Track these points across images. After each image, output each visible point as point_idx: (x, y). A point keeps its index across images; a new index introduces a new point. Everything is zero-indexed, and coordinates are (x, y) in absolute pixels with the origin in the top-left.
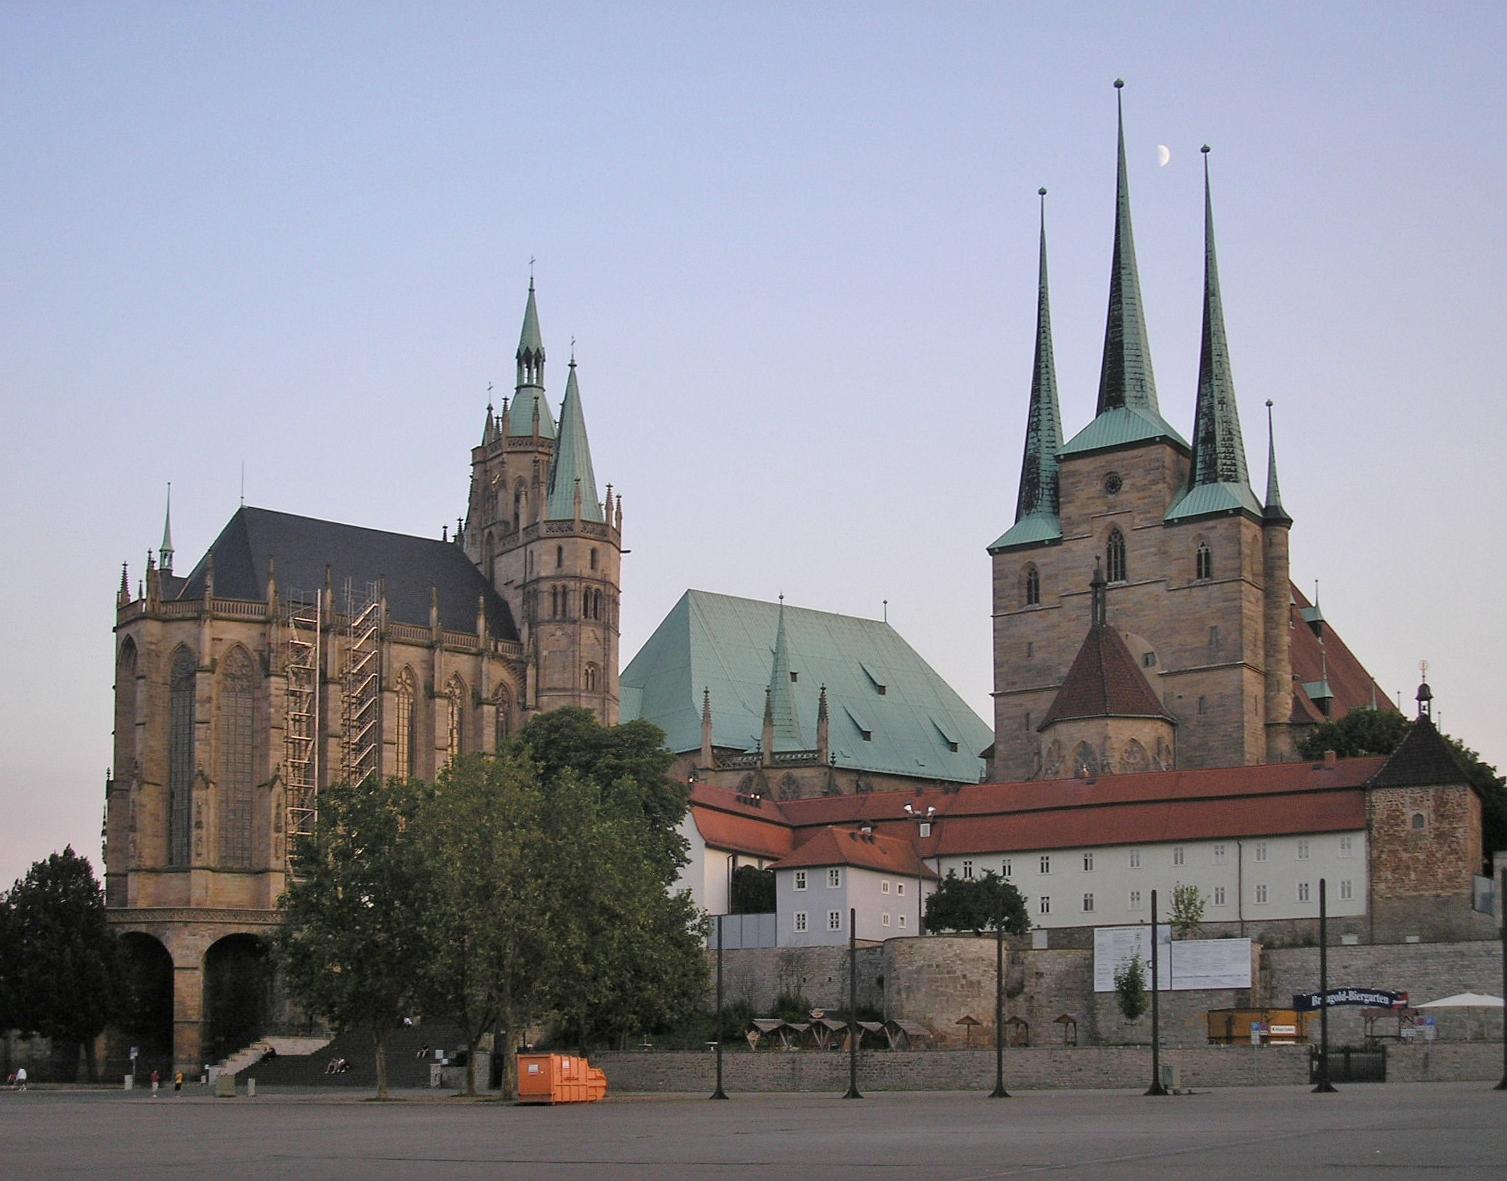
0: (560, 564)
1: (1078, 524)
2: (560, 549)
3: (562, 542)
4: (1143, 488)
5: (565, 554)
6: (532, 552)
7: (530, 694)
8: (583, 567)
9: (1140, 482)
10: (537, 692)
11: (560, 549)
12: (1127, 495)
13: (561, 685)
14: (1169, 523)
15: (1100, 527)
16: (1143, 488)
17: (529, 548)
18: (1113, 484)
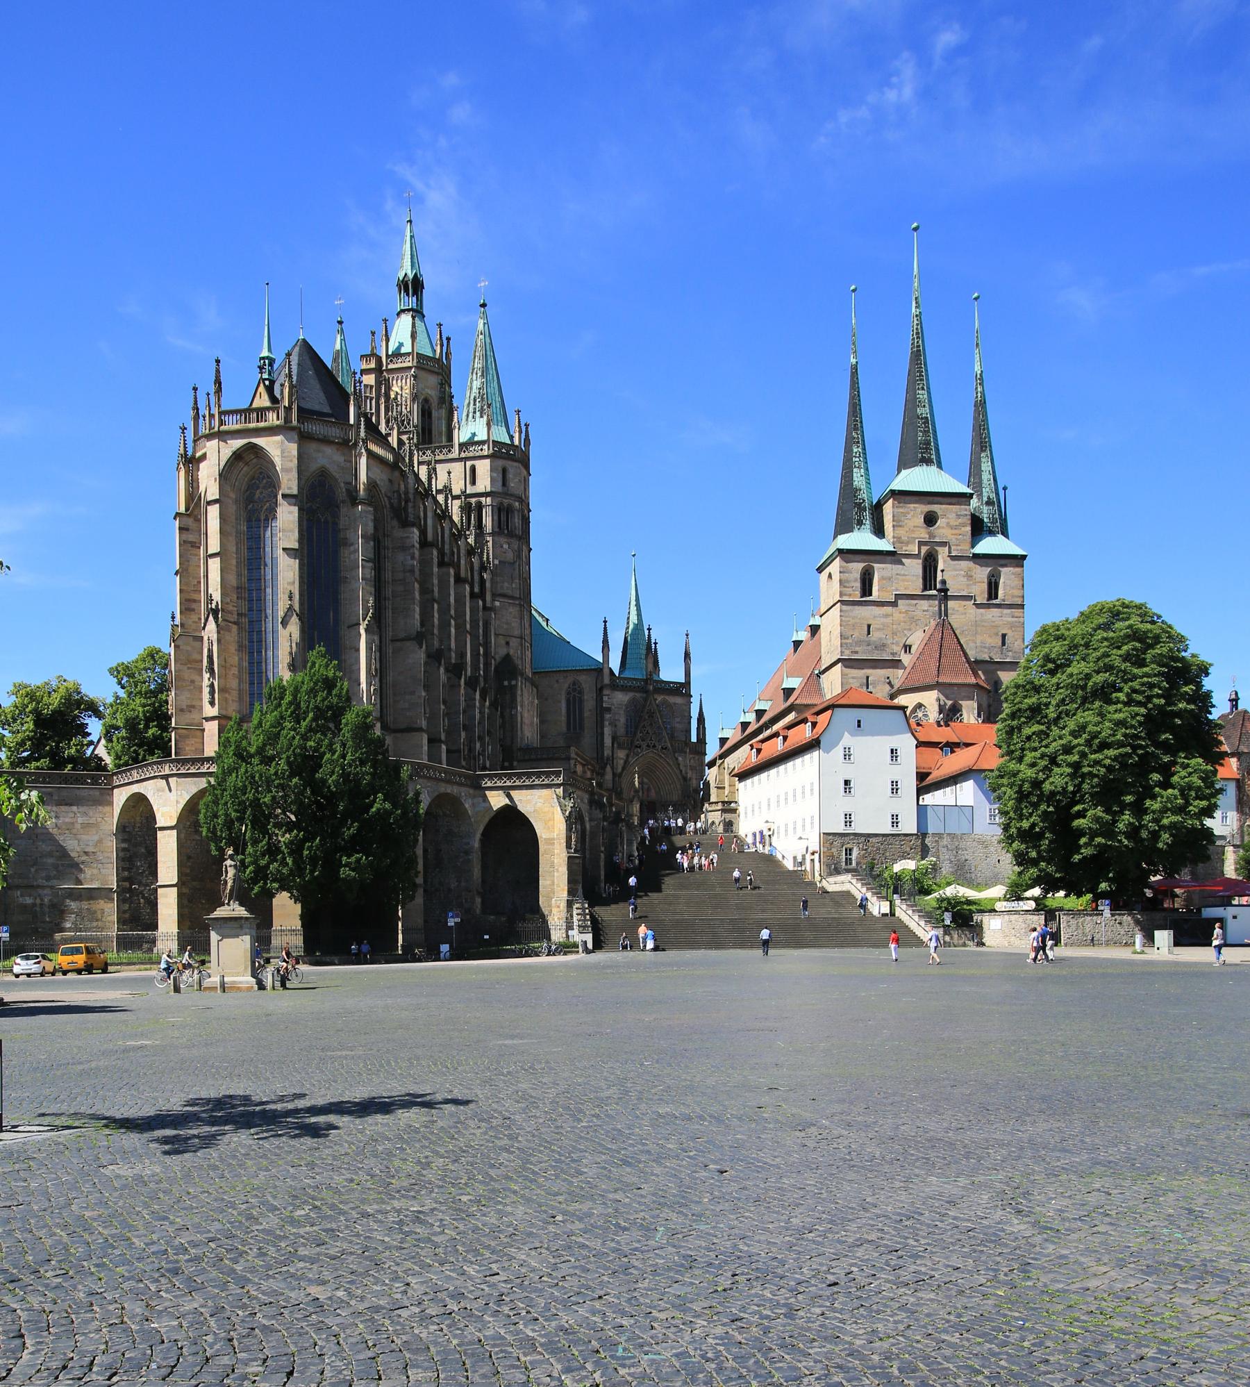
0: (504, 484)
1: (907, 543)
2: (504, 471)
3: (508, 464)
4: (956, 527)
5: (510, 476)
6: (473, 469)
7: (488, 597)
8: (519, 492)
9: (953, 523)
10: (494, 596)
11: (504, 471)
12: (942, 530)
13: (510, 592)
14: (977, 558)
15: (924, 549)
16: (956, 527)
17: (469, 464)
18: (930, 520)
